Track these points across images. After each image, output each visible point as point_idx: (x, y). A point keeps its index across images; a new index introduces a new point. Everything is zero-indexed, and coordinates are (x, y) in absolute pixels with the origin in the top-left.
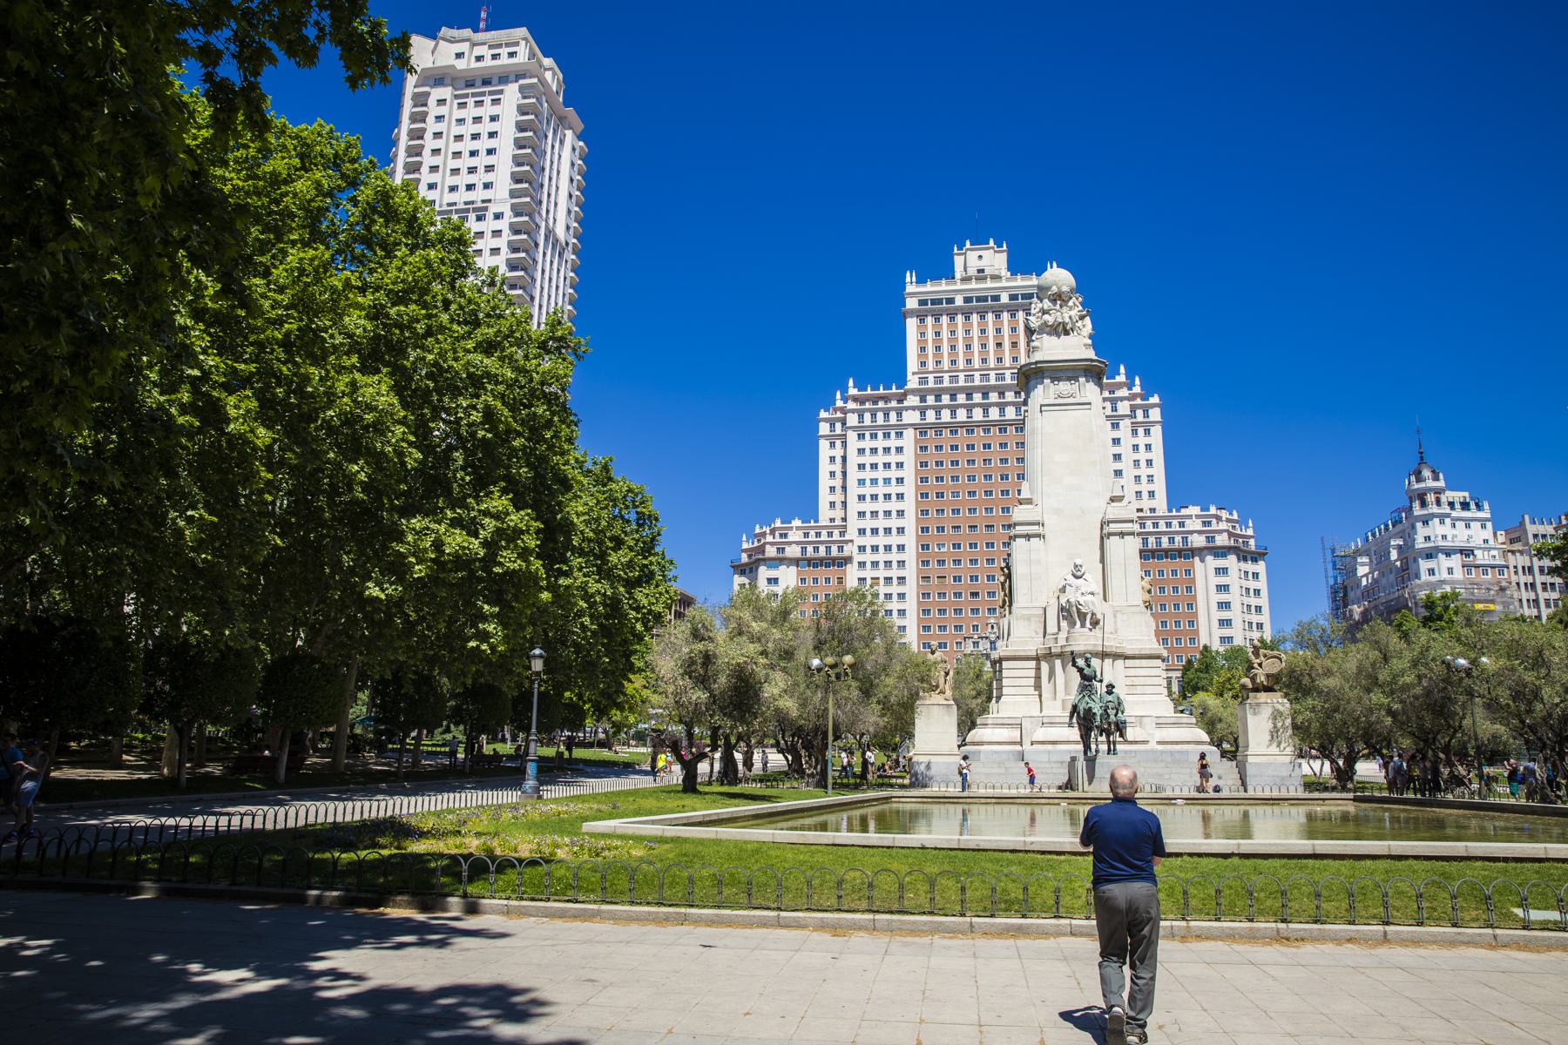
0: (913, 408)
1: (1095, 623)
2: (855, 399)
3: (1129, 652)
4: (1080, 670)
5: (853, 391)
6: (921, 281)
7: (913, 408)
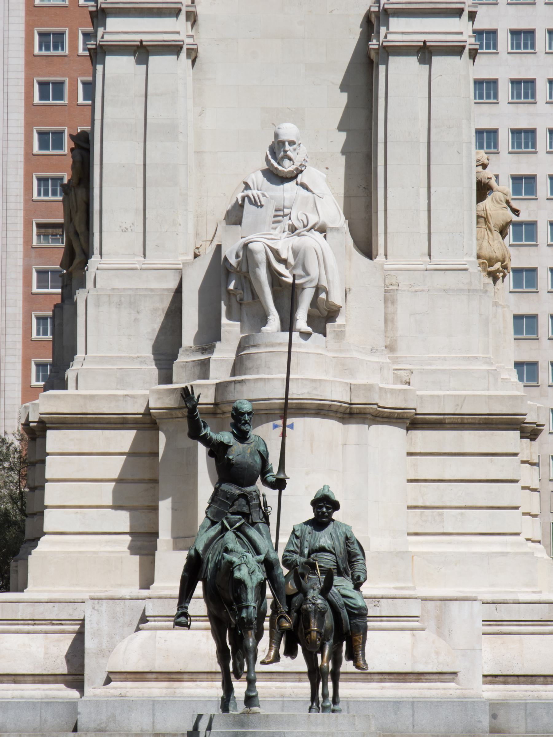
3: (427, 408)
4: (218, 451)
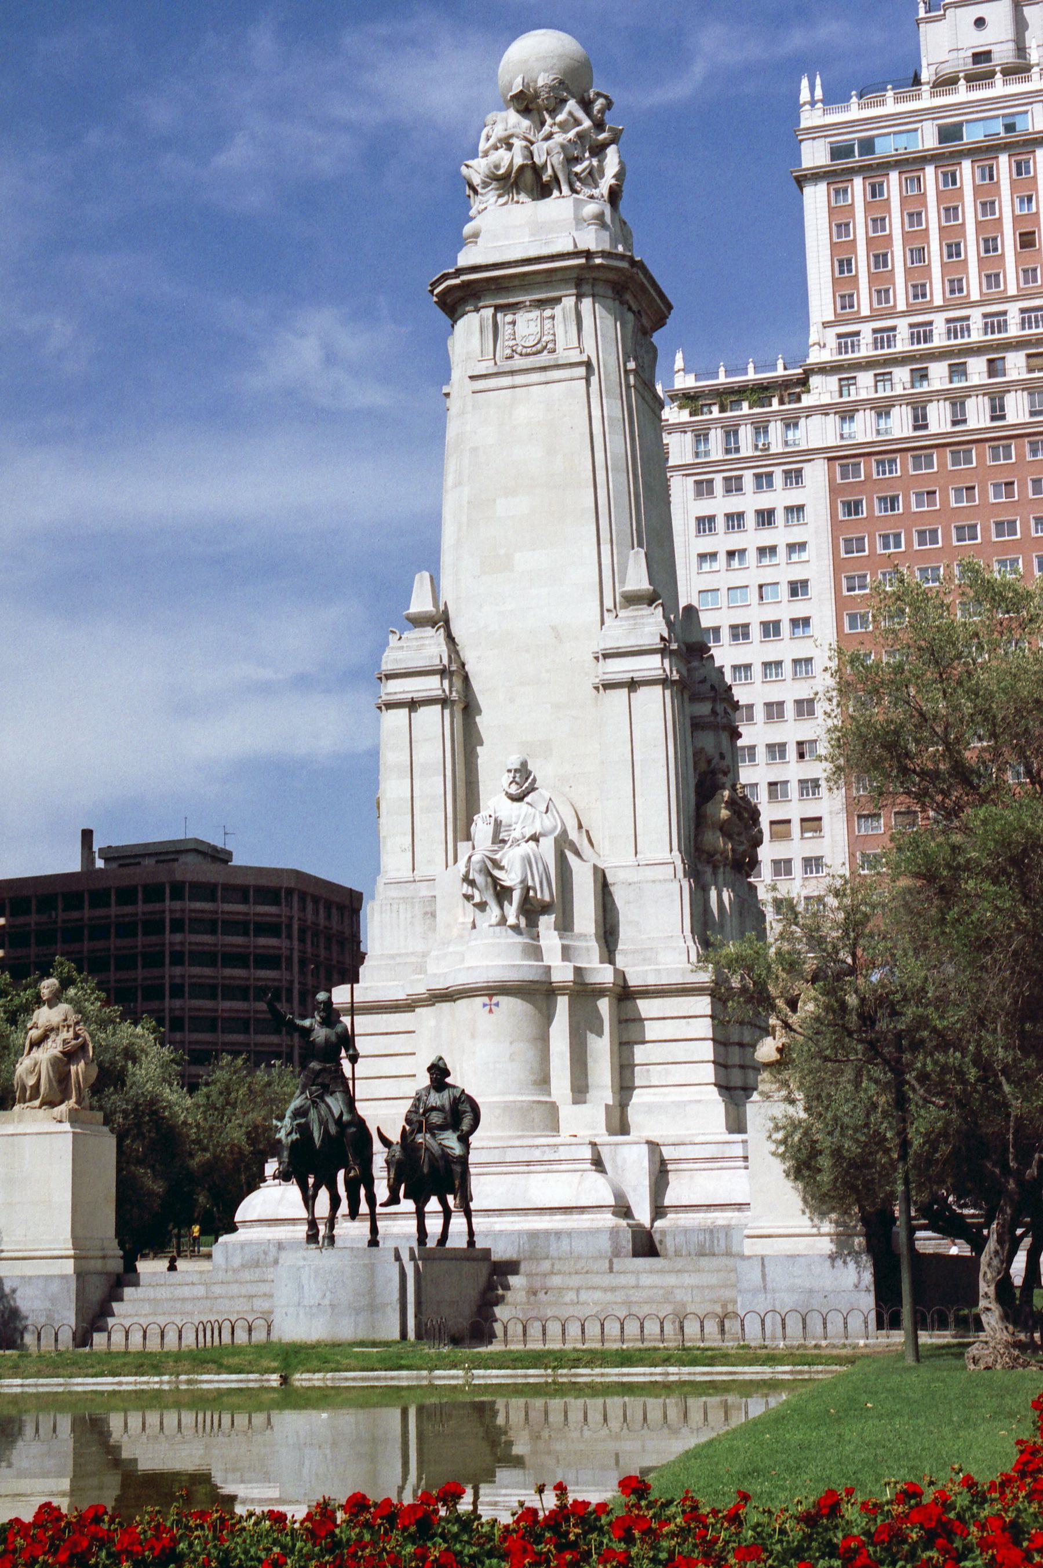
0: (824, 410)
1: (532, 910)
2: (690, 399)
5: (685, 382)
6: (834, 98)
7: (824, 410)
